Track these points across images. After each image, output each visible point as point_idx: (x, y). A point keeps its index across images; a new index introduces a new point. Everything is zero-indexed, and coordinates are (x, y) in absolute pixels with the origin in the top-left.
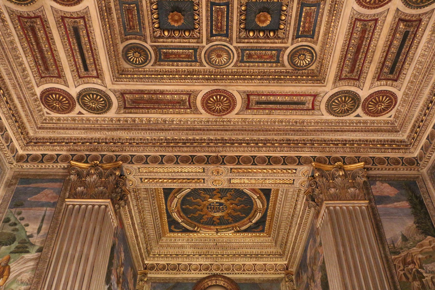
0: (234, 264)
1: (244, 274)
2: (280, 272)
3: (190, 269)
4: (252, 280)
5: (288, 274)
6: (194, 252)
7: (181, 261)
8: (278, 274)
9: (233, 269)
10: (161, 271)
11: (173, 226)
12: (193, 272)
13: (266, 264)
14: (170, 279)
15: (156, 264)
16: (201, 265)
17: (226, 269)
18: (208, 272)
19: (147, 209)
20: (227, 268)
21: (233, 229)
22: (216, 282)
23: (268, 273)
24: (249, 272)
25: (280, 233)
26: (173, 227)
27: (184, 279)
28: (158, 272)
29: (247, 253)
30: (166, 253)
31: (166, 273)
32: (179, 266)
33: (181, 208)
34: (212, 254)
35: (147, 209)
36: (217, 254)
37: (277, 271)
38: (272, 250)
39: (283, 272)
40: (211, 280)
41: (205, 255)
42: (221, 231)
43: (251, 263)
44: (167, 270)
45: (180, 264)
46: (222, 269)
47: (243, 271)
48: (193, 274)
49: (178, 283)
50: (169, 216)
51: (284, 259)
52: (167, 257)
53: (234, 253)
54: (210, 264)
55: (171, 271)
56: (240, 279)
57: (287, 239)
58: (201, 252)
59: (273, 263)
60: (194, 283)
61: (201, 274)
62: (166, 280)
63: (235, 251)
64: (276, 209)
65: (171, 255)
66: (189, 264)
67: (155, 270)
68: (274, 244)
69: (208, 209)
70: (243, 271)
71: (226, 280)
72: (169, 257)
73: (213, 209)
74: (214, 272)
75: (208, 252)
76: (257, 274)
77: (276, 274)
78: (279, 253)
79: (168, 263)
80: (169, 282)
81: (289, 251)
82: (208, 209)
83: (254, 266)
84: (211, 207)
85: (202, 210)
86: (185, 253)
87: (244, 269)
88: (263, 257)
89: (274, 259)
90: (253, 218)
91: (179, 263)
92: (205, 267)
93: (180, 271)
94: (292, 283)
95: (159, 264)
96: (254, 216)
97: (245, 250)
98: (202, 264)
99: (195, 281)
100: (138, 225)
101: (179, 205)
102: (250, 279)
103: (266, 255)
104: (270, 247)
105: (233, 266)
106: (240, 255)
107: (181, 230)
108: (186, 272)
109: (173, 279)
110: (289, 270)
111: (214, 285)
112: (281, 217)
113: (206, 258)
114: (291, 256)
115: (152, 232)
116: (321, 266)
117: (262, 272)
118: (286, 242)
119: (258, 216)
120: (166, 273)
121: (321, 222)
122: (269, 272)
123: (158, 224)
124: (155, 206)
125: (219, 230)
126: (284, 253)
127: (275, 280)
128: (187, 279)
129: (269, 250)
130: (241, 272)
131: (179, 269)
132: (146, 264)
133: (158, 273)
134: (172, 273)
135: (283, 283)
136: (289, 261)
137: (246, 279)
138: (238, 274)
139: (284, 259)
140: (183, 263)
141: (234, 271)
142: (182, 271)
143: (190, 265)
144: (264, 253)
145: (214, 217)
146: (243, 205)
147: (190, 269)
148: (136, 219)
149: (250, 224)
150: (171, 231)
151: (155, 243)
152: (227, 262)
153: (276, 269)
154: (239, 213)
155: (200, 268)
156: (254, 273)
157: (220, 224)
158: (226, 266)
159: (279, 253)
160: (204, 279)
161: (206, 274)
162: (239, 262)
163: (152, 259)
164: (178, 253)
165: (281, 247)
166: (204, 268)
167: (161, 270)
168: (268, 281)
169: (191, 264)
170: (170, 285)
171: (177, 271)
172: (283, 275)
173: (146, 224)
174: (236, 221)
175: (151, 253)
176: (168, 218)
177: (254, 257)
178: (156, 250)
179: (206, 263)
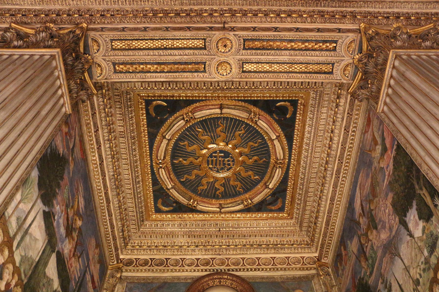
0: (245, 258)
1: (259, 270)
2: (309, 266)
3: (182, 264)
4: (271, 278)
5: (321, 266)
6: (188, 243)
7: (171, 255)
8: (307, 269)
9: (243, 263)
10: (141, 268)
11: (160, 201)
12: (187, 267)
13: (289, 257)
14: (154, 278)
15: (136, 259)
16: (198, 259)
17: (234, 264)
18: (208, 267)
19: (124, 156)
20: (234, 262)
21: (242, 203)
22: (220, 282)
23: (292, 269)
24: (267, 267)
25: (308, 204)
26: (160, 201)
27: (174, 278)
28: (137, 268)
29: (262, 243)
30: (149, 245)
31: (149, 270)
32: (167, 261)
33: (173, 164)
34: (214, 244)
35: (124, 156)
36: (221, 244)
37: (305, 265)
38: (296, 238)
39: (314, 266)
40: (213, 279)
41: (204, 246)
42: (226, 206)
43: (269, 256)
44: (150, 266)
45: (169, 259)
46: (228, 264)
47: (257, 265)
48: (187, 271)
49: (165, 283)
50: (155, 181)
51: (314, 249)
52: (150, 250)
53: (244, 243)
54: (211, 259)
55: (157, 267)
56: (254, 278)
57: (318, 211)
58: (198, 243)
59: (298, 256)
60: (188, 283)
61: (198, 271)
62: (149, 279)
63: (245, 241)
64: (302, 162)
65: (156, 246)
66: (181, 259)
67: (134, 266)
68: (298, 229)
69: (208, 165)
70: (257, 265)
71: (234, 279)
72: (153, 250)
73: (216, 165)
74: (217, 267)
75: (209, 242)
76: (277, 269)
77: (303, 269)
78: (306, 243)
79: (152, 257)
80: (152, 283)
81: (321, 231)
82: (208, 165)
83: (273, 260)
84: (212, 160)
85: (199, 167)
86: (176, 244)
87: (259, 263)
88: (284, 248)
89: (300, 249)
90: (270, 181)
91: (167, 257)
92: (204, 262)
93: (168, 266)
94: (328, 277)
95: (139, 259)
96: (271, 177)
97: (258, 239)
98: (199, 259)
99: (189, 281)
100: (110, 180)
101: (168, 158)
102: (268, 277)
103: (288, 244)
104: (293, 233)
105: (243, 260)
106: (252, 245)
107: (171, 208)
108: (177, 268)
109: (158, 279)
110: (323, 261)
111: (217, 286)
112: (308, 174)
113: (206, 250)
114: (322, 245)
115: (132, 213)
116: (390, 182)
117: (285, 266)
118: (317, 218)
119: (278, 174)
120: (149, 270)
121: (388, 95)
122: (294, 266)
123: (140, 192)
124: (135, 155)
125: (223, 206)
126: (312, 241)
127: (303, 277)
128: (179, 278)
129: (292, 239)
130: (255, 267)
131: (167, 264)
132: (120, 259)
133: (138, 271)
134: (156, 270)
135: (316, 280)
136: (321, 251)
137: (262, 278)
138: (251, 270)
139: (314, 249)
140: (174, 257)
141: (245, 266)
142: (172, 267)
143: (183, 260)
144: (285, 243)
145: (216, 180)
146: (255, 158)
147: (182, 264)
148: (108, 168)
149: (267, 191)
150: (158, 211)
151: (134, 227)
152: (234, 256)
153: (303, 262)
154: (250, 173)
155: (197, 263)
156: (274, 269)
157: (225, 195)
158: (233, 261)
159: (306, 243)
160: (203, 277)
161: (206, 271)
162: (252, 255)
163: (129, 252)
164: (166, 244)
165: (308, 231)
166: (202, 263)
167: (141, 266)
168: (294, 279)
169: (184, 259)
170: (154, 286)
171: (165, 266)
172: (314, 272)
173: (122, 186)
174: (246, 190)
175: (129, 244)
176: (153, 185)
177: (271, 248)
178: (136, 241)
179: (206, 257)
